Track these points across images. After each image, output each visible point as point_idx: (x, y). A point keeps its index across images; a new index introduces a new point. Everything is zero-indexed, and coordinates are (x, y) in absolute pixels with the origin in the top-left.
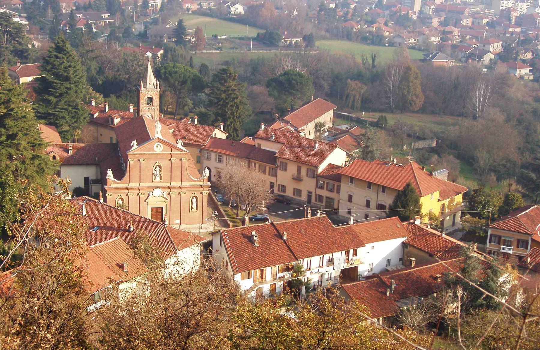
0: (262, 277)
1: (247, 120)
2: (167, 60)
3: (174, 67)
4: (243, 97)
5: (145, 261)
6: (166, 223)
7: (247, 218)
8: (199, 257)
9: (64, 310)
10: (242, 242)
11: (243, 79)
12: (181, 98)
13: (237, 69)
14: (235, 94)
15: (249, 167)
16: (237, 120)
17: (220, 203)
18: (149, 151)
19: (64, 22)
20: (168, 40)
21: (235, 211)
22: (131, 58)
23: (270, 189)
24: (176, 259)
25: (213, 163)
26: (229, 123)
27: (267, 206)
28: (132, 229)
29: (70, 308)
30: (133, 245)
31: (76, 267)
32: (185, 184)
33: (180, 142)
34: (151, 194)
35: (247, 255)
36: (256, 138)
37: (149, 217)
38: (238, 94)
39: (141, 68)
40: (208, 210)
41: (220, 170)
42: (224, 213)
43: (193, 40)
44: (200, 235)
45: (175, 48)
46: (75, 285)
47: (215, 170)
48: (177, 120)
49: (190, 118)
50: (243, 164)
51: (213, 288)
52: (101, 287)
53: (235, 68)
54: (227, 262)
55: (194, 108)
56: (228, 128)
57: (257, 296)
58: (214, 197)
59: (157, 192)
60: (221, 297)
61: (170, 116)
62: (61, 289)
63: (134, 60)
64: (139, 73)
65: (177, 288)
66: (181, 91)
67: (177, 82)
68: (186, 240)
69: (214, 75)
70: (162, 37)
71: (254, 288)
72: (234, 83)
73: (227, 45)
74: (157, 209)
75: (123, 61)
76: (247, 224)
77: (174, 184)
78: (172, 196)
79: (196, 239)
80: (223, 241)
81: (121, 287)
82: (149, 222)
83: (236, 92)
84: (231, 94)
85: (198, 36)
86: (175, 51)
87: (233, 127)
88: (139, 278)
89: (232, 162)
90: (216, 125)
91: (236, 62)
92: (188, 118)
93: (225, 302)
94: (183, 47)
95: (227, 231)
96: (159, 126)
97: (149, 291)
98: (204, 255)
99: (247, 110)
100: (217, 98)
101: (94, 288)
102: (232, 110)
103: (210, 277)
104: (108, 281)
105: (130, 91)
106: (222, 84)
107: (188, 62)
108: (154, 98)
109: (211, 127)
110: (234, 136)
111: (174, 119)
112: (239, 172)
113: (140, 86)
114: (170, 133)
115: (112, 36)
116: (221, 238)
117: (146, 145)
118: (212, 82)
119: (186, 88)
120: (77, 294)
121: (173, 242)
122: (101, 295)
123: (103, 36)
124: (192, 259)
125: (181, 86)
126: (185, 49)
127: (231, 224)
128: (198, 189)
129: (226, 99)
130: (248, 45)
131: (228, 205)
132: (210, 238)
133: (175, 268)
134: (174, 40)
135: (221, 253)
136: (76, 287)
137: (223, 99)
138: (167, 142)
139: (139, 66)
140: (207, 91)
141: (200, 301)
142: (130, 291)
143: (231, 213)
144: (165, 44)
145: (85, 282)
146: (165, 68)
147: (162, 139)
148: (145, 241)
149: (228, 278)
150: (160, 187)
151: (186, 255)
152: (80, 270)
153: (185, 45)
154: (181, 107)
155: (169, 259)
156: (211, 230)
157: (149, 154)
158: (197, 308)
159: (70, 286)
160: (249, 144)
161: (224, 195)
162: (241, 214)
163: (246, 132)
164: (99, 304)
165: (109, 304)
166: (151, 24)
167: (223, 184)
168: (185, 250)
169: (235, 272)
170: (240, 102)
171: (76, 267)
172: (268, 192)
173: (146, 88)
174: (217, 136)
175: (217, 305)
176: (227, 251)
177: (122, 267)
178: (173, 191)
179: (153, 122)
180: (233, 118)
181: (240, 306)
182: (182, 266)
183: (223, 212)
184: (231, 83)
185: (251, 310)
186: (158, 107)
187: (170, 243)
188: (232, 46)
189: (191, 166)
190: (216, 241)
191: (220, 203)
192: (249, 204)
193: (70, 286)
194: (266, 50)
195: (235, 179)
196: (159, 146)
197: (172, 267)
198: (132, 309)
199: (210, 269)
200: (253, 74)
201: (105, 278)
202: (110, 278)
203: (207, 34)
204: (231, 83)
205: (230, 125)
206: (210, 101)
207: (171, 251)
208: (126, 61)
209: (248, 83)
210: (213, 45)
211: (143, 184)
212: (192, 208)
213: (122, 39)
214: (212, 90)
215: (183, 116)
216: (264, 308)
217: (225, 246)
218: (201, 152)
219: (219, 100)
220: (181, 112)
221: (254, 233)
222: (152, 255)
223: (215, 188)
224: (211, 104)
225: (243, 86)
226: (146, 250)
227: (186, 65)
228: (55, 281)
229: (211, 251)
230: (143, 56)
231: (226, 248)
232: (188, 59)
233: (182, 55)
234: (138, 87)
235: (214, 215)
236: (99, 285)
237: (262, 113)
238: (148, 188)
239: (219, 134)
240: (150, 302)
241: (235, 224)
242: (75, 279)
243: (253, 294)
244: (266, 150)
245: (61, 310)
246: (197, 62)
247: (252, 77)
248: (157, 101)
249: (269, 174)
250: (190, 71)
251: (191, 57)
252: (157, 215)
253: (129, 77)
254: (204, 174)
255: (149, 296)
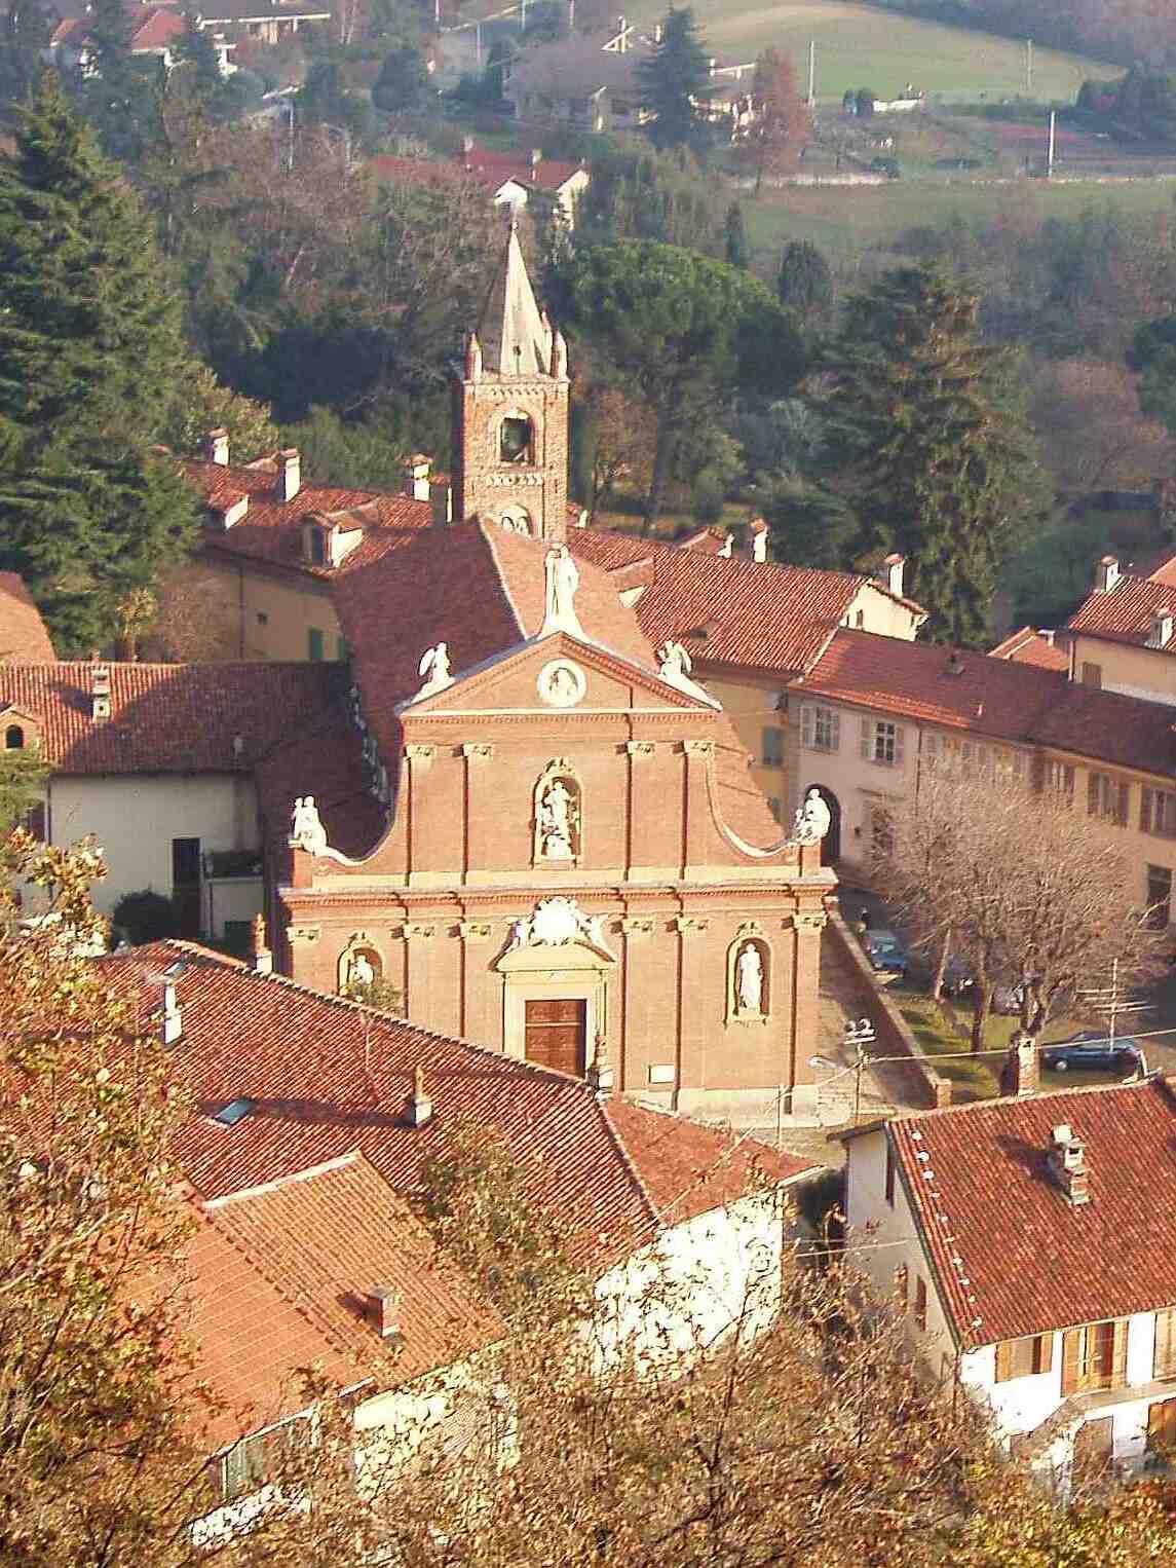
0: (1106, 1368)
1: (1025, 542)
2: (606, 224)
3: (643, 259)
4: (1008, 420)
5: (493, 1283)
6: (604, 1081)
7: (1027, 1057)
8: (776, 1261)
9: (67, 1539)
10: (999, 1184)
11: (1005, 324)
12: (679, 424)
13: (972, 273)
14: (964, 402)
15: (1038, 786)
16: (972, 541)
17: (885, 977)
18: (514, 704)
19: (66, 25)
20: (615, 119)
21: (965, 1019)
22: (420, 214)
23: (1151, 902)
24: (653, 1270)
25: (849, 766)
26: (931, 554)
27: (1133, 994)
28: (423, 1113)
29: (97, 1528)
30: (427, 1198)
31: (128, 1313)
32: (702, 874)
33: (676, 653)
34: (522, 931)
35: (1029, 1251)
36: (1077, 634)
37: (515, 1049)
38: (980, 402)
39: (472, 268)
40: (820, 1013)
41: (885, 804)
42: (905, 1029)
43: (745, 119)
44: (784, 1147)
45: (648, 163)
46: (124, 1410)
47: (859, 799)
48: (661, 539)
49: (730, 529)
50: (1008, 768)
51: (847, 1422)
52: (258, 1417)
53: (963, 268)
54: (922, 1288)
55: (750, 478)
56: (927, 582)
57: (1079, 1462)
58: (854, 947)
59: (558, 920)
60: (889, 1469)
61: (621, 520)
62: (51, 1429)
63: (436, 227)
64: (459, 293)
65: (658, 1424)
66: (682, 387)
67: (660, 342)
68: (706, 1170)
69: (856, 305)
70: (580, 105)
71: (1067, 1421)
72: (960, 345)
73: (921, 143)
74: (554, 1007)
75: (375, 229)
76: (1030, 1088)
77: (641, 876)
78: (636, 938)
79: (759, 1164)
80: (904, 1177)
81: (366, 1415)
82: (510, 1077)
83: (967, 393)
84: (944, 403)
85: (772, 98)
86: (648, 179)
87: (953, 580)
88: (460, 1369)
89: (948, 760)
90: (863, 565)
91: (969, 235)
92: (719, 529)
93: (911, 1494)
94: (689, 157)
95: (921, 1125)
96: (566, 572)
97: (511, 1440)
98: (802, 1248)
99: (1027, 490)
100: (868, 426)
101: (225, 1426)
102: (948, 487)
103: (833, 1367)
104: (298, 1384)
105: (414, 391)
106: (897, 354)
107: (719, 234)
108: (539, 425)
109: (837, 578)
110: (959, 625)
111: (644, 533)
112: (977, 806)
113: (465, 360)
114: (621, 609)
115: (320, 100)
116: (892, 1161)
117: (498, 674)
118: (840, 337)
119: (708, 373)
120: (133, 1453)
121: (639, 1180)
122: (259, 1459)
123: (274, 101)
124: (741, 1269)
125: (683, 359)
126: (702, 165)
127: (943, 1086)
128: (770, 905)
129: (919, 428)
130: (1030, 143)
131: (926, 987)
132: (833, 1160)
133: (650, 1319)
134: (643, 117)
135: (889, 1239)
136: (129, 1418)
137: (898, 428)
138: (606, 657)
139: (460, 256)
140: (818, 386)
141: (779, 1491)
142: (416, 1438)
143: (942, 1028)
144: (597, 141)
145: (175, 1391)
146: (600, 268)
147: (586, 640)
148: (490, 1177)
149: (929, 1373)
150: (569, 895)
151: (709, 1252)
152: (152, 1326)
153: (702, 149)
154: (680, 472)
155: (615, 1273)
156: (841, 1116)
157: (514, 719)
158: (766, 1526)
159: (97, 1414)
160: (1036, 669)
161: (905, 932)
162: (996, 1033)
163: (1020, 602)
164: (251, 1507)
165: (305, 1505)
166: (524, 35)
167: (901, 876)
168: (700, 1224)
169: (966, 1340)
170: (991, 447)
171: (128, 1313)
172: (1138, 916)
173: (495, 370)
174: (868, 626)
175: (872, 1510)
176: (920, 1227)
177: (369, 1311)
178: (639, 914)
179: (531, 548)
180: (955, 529)
181: (991, 1520)
182: (689, 1305)
183: (900, 1022)
184: (945, 347)
185: (1047, 1536)
186: (561, 474)
187: (622, 1188)
188: (948, 151)
189: (733, 779)
190: (867, 1177)
191: (885, 977)
192: (1036, 983)
193: (97, 1414)
194: (1129, 172)
195: (967, 850)
196: (562, 675)
197: (634, 1310)
198: (425, 1533)
199: (835, 1324)
200: (1056, 297)
201: (283, 1372)
202: (309, 1372)
203: (817, 87)
204: (945, 347)
205: (936, 567)
206: (835, 441)
207: (628, 1229)
208: (391, 230)
209: (1032, 349)
210: (850, 146)
211: (479, 879)
212: (740, 1002)
213: (372, 114)
214: (844, 380)
215: (690, 522)
216: (1119, 1530)
217: (911, 1201)
218: (787, 709)
219: (884, 433)
220: (682, 496)
221: (1063, 1134)
222: (530, 1251)
223: (861, 896)
224: (835, 455)
225: (1009, 361)
226: (497, 1225)
227: (708, 251)
228: (20, 1385)
229: (837, 1230)
230: (483, 204)
231: (915, 1211)
232: (720, 220)
233: (685, 200)
234: (457, 367)
235: (852, 1038)
236: (250, 1407)
237: (1108, 501)
238: (508, 897)
239: (881, 612)
240: (518, 1499)
241: (962, 1087)
242: (125, 1378)
243: (1060, 1452)
244: (1141, 704)
245: (52, 1536)
246: (764, 234)
247: (1055, 315)
248: (553, 443)
249: (1144, 826)
250: (726, 282)
251: (734, 213)
252: (553, 1039)
253: (411, 315)
254: (804, 826)
255: (512, 1462)
